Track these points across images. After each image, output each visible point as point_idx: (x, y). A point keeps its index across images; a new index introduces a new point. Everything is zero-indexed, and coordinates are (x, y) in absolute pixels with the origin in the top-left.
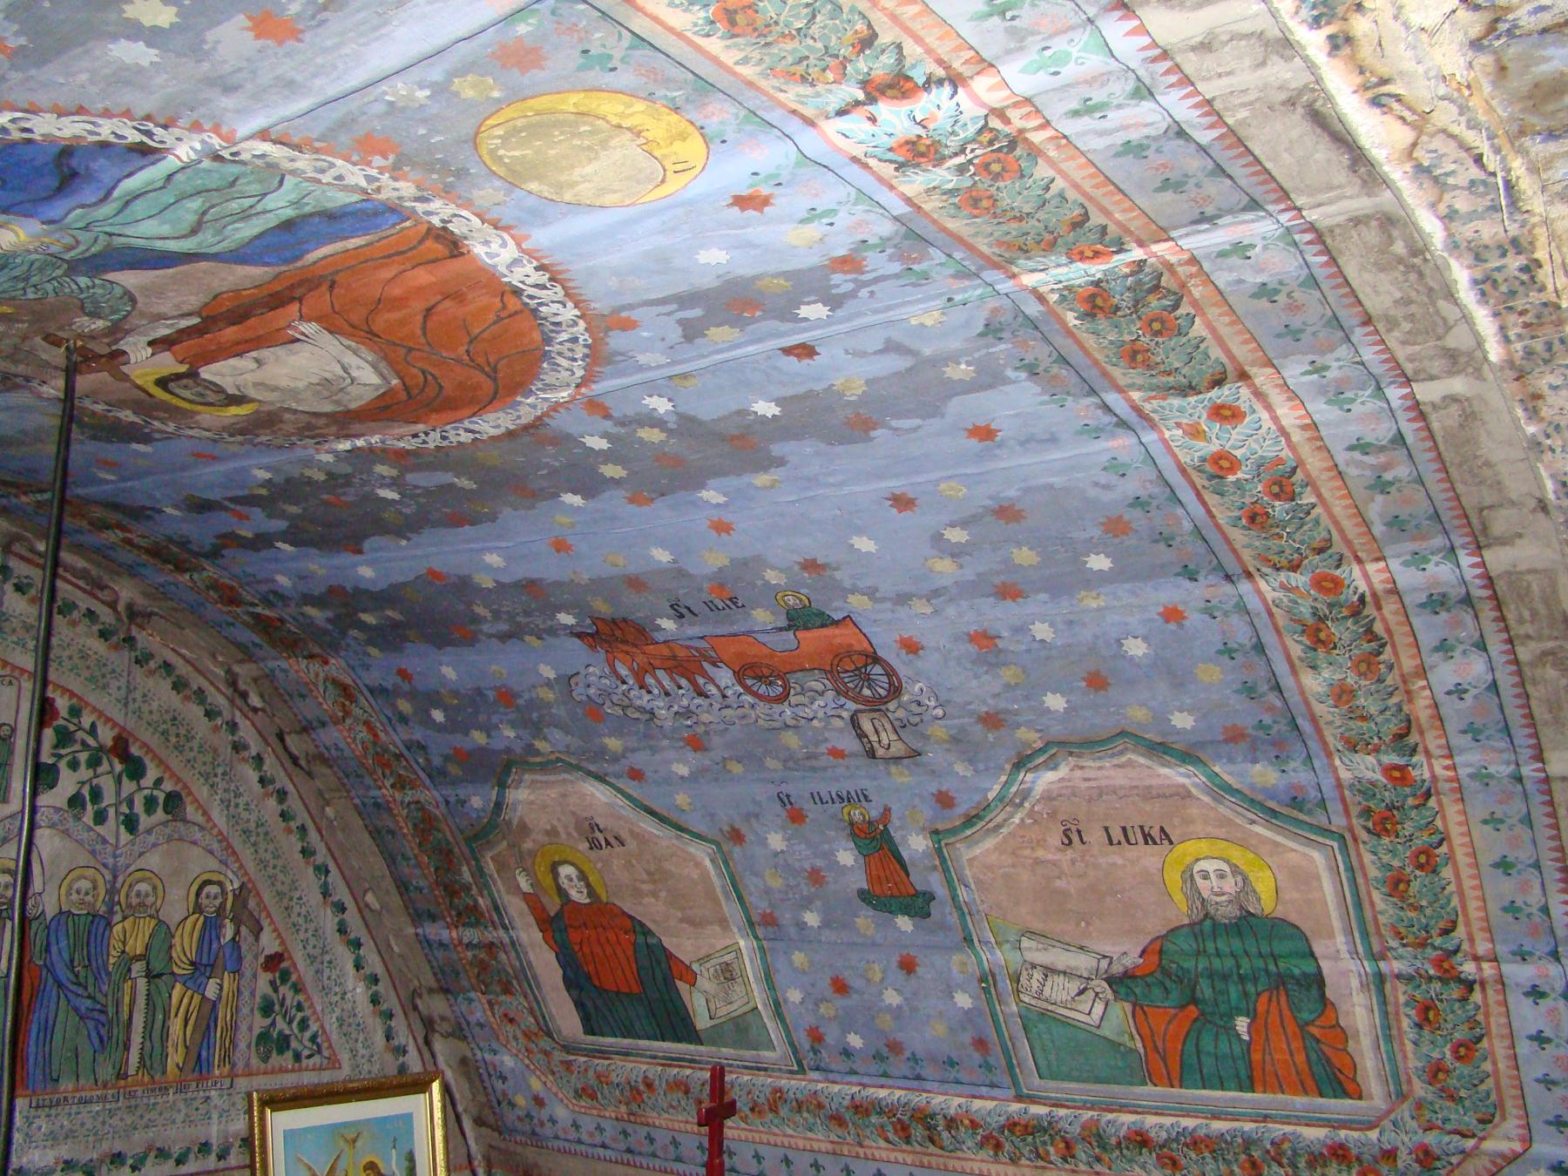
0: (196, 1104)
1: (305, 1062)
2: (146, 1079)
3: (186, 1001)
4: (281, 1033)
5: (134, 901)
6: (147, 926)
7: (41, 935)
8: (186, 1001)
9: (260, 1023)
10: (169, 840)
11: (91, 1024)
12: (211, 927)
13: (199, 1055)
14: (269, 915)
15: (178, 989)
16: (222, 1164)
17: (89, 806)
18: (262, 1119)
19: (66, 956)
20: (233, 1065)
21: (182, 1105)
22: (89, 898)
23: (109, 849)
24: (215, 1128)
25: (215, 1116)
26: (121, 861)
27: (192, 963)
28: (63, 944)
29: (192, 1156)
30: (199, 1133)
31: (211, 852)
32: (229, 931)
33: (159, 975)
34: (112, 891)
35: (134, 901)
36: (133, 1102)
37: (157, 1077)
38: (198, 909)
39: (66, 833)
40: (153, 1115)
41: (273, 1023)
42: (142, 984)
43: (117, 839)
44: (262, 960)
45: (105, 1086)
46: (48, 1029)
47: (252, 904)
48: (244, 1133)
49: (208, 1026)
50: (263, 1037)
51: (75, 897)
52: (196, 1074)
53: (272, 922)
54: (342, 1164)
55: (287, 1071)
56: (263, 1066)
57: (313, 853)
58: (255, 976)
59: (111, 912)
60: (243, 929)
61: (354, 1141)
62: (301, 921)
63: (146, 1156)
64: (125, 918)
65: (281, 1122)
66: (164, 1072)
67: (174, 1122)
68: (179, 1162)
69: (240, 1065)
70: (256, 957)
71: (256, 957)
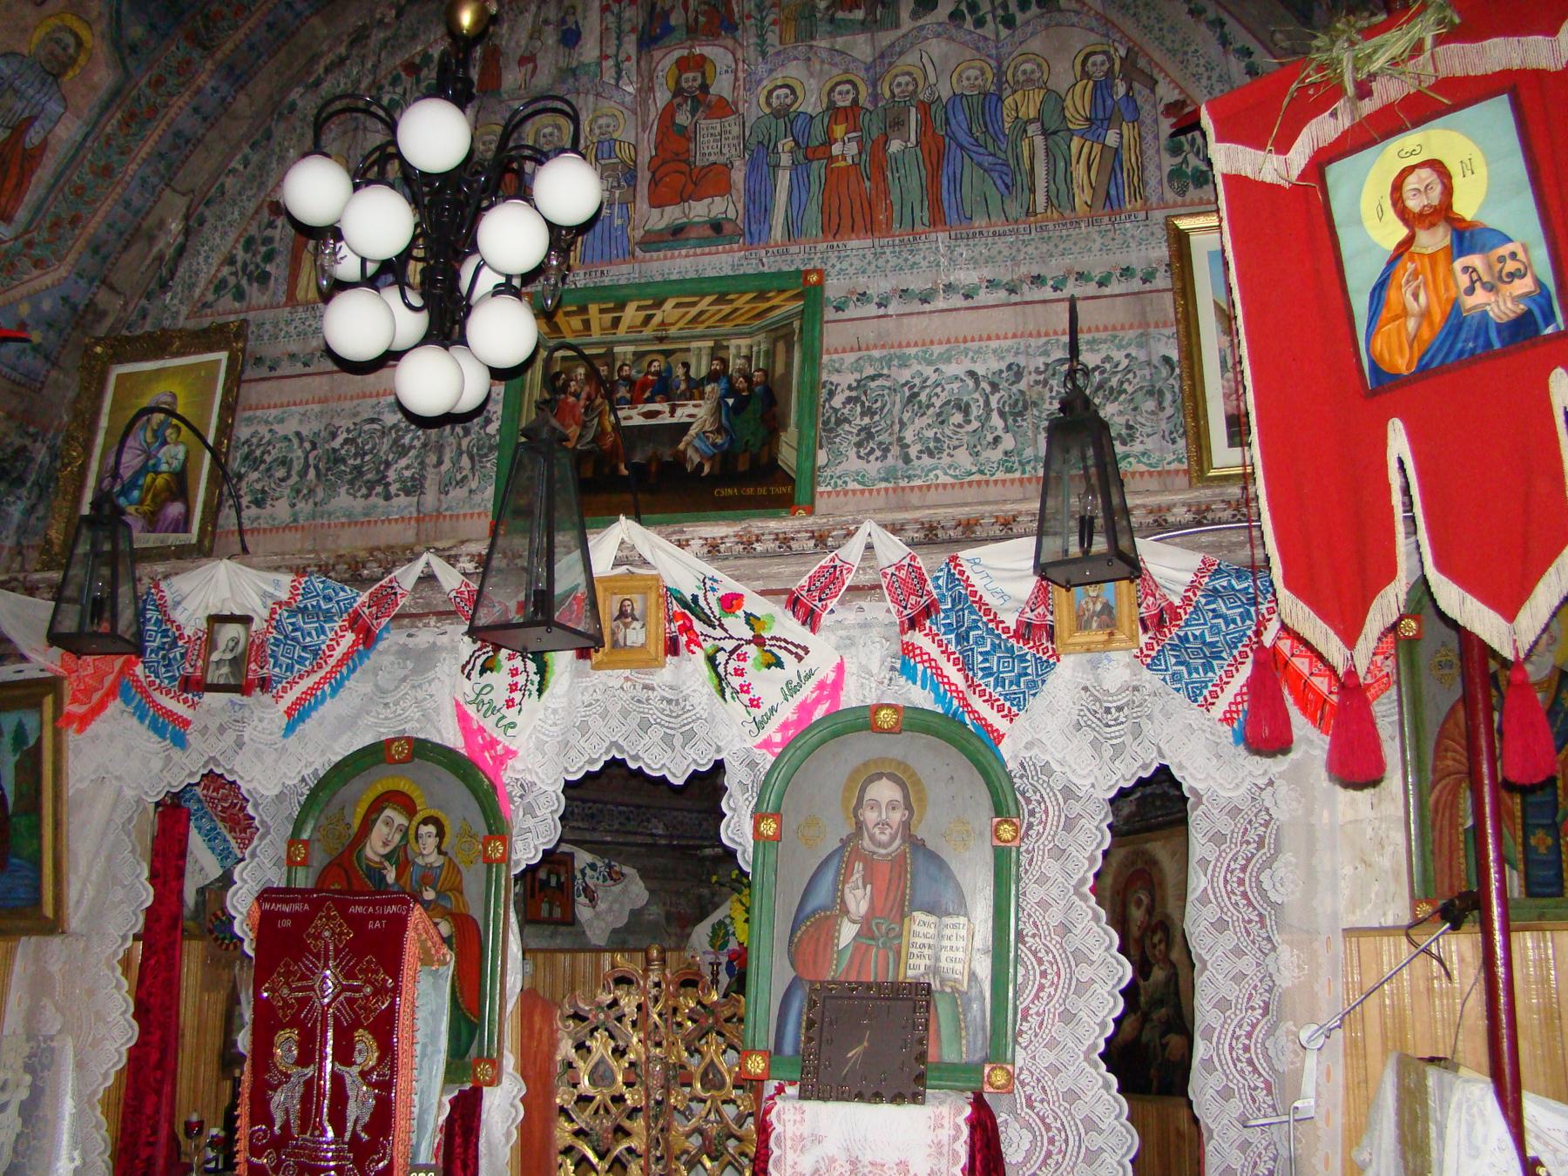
2: (1056, 215)
3: (1085, 150)
4: (1196, 169)
5: (1021, 78)
6: (1037, 97)
7: (940, 116)
8: (1085, 150)
9: (1169, 162)
10: (1047, 26)
11: (995, 175)
12: (1102, 88)
13: (1108, 195)
14: (1162, 70)
15: (1075, 143)
17: (968, 17)
19: (964, 126)
20: (1146, 200)
21: (1096, 236)
22: (979, 81)
23: (991, 44)
26: (1003, 50)
27: (1087, 119)
28: (961, 117)
30: (1122, 259)
31: (1092, 30)
32: (1121, 89)
33: (1055, 133)
34: (1000, 74)
35: (1021, 78)
37: (1067, 213)
38: (1085, 74)
39: (951, 39)
40: (1067, 245)
41: (1185, 160)
42: (1039, 141)
43: (997, 35)
44: (1161, 108)
45: (1016, 221)
46: (956, 182)
47: (1142, 63)
49: (1113, 169)
50: (1176, 174)
51: (965, 83)
52: (1108, 209)
53: (1167, 75)
56: (1179, 199)
57: (1205, 11)
58: (1156, 121)
59: (1000, 89)
60: (1136, 85)
62: (1201, 70)
63: (1065, 279)
64: (1014, 92)
66: (1073, 209)
67: (1090, 250)
68: (1101, 284)
69: (1154, 200)
70: (1155, 106)
71: (1155, 106)
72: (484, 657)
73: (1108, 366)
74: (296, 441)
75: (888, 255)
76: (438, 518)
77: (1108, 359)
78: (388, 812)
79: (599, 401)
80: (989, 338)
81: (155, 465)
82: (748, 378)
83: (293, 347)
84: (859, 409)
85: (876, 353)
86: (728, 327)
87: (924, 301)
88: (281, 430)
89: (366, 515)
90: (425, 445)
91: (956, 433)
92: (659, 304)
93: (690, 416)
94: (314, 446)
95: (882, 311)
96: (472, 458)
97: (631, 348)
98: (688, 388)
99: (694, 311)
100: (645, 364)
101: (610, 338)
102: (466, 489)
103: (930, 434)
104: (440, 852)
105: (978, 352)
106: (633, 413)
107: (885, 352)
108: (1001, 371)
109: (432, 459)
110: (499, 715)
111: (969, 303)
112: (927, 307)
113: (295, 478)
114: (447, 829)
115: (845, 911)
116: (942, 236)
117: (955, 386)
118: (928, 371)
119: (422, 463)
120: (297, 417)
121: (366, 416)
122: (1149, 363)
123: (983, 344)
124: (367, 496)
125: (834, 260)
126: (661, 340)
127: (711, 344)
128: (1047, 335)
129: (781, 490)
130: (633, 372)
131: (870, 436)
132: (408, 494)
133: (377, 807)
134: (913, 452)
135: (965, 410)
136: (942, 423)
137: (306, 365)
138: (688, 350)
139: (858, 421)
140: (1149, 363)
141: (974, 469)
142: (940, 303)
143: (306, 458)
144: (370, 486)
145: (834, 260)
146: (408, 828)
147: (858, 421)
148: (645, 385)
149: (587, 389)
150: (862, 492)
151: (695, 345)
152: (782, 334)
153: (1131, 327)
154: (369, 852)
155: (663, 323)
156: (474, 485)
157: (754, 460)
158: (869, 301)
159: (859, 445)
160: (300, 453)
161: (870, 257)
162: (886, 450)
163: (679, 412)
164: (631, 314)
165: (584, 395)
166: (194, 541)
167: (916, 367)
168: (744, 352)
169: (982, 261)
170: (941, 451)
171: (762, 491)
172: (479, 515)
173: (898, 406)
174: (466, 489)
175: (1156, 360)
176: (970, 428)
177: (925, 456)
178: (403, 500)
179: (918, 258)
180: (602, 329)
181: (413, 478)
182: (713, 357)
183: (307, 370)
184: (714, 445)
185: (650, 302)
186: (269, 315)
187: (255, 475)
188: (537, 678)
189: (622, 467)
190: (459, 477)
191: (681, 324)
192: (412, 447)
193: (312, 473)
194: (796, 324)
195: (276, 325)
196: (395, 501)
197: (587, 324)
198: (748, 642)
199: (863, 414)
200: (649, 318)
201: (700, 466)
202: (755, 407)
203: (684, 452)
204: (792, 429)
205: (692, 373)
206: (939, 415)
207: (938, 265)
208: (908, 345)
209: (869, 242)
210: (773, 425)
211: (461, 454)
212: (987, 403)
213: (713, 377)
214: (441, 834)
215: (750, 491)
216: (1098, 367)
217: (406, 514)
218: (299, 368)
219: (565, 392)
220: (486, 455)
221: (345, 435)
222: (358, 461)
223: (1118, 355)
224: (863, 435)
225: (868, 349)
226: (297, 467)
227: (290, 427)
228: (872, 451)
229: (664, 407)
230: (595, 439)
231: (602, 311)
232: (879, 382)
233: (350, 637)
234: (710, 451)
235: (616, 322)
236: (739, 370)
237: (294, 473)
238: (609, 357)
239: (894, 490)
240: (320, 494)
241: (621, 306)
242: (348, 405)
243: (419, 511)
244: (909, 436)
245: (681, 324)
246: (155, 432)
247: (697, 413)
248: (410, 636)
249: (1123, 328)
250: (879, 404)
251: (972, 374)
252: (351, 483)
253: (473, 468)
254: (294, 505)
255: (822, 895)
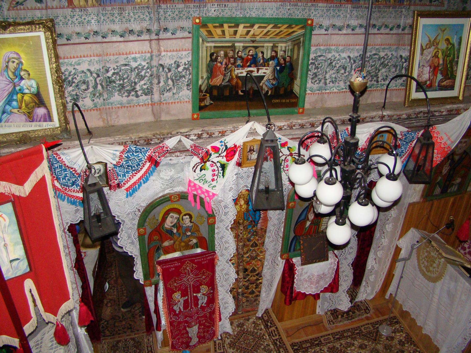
0: (398, 12)
1: (433, 3)
2: (384, 3)
16: (403, 32)
18: (417, 20)
21: (393, 12)
24: (402, 21)
25: (403, 17)
29: (394, 29)
36: (380, 10)
40: (385, 14)
48: (411, 23)
54: (438, 38)
55: (427, 5)
56: (419, 3)
61: (444, 31)
63: (382, 26)
65: (423, 21)
68: (391, 30)
72: (201, 165)
73: (386, 57)
74: (89, 74)
75: (331, 11)
76: (160, 104)
77: (386, 55)
78: (171, 214)
79: (230, 66)
80: (356, 45)
81: (20, 90)
82: (285, 59)
83: (78, 29)
84: (314, 67)
85: (322, 48)
86: (278, 39)
87: (340, 30)
88: (80, 68)
89: (128, 103)
90: (151, 75)
91: (341, 76)
92: (252, 26)
93: (264, 73)
94: (98, 76)
95: (326, 32)
96: (173, 81)
97: (242, 44)
98: (264, 62)
99: (266, 30)
100: (247, 51)
101: (233, 39)
102: (171, 93)
103: (334, 76)
104: (191, 222)
105: (352, 50)
106: (243, 71)
107: (325, 47)
108: (357, 57)
109: (155, 81)
110: (209, 184)
111: (353, 32)
112: (340, 32)
113: (91, 89)
114: (193, 216)
115: (308, 219)
116: (350, 6)
117: (344, 60)
118: (337, 55)
119: (151, 83)
120: (87, 63)
121: (122, 63)
122: (396, 57)
123: (354, 47)
124: (128, 96)
125: (313, 11)
126: (253, 42)
127: (272, 45)
128: (372, 45)
129: (294, 100)
130: (243, 54)
131: (316, 76)
132: (146, 95)
133: (167, 213)
134: (328, 82)
135: (345, 68)
136: (338, 73)
137: (86, 38)
138: (263, 47)
139: (313, 71)
140: (396, 57)
141: (344, 88)
142: (344, 32)
143: (95, 80)
144: (129, 92)
145: (313, 11)
146: (179, 218)
147: (313, 71)
148: (248, 60)
149: (225, 60)
150: (311, 94)
151: (266, 45)
152: (297, 43)
153: (395, 45)
154: (166, 226)
155: (254, 35)
156: (175, 91)
157: (286, 89)
158: (322, 28)
159: (312, 79)
160: (91, 78)
161: (325, 11)
162: (320, 81)
163: (260, 71)
164: (241, 29)
165: (224, 63)
166: (58, 125)
167: (333, 53)
168: (283, 49)
169: (360, 17)
170: (336, 81)
171: (288, 101)
172: (178, 102)
173: (326, 66)
174: (171, 93)
175: (398, 56)
176: (345, 75)
177: (331, 83)
178: (144, 97)
179: (340, 13)
180: (230, 35)
181: (147, 88)
182: (272, 50)
183: (87, 41)
184: (272, 84)
185: (249, 25)
186: (60, 12)
187: (71, 89)
188: (222, 171)
189: (240, 92)
190: (168, 88)
191: (261, 36)
192: (145, 76)
193: (99, 87)
194: (302, 39)
195: (65, 18)
196: (141, 98)
197: (223, 32)
198: (288, 156)
199: (315, 69)
200: (248, 32)
201: (268, 92)
202: (286, 71)
203: (262, 87)
204: (298, 79)
205: (265, 56)
206: (337, 70)
207: (346, 17)
208: (332, 45)
209: (325, 4)
210: (292, 78)
211: (168, 79)
212: (352, 67)
213: (272, 58)
214: (191, 217)
215: (284, 101)
216: (383, 57)
217: (146, 102)
218: (83, 40)
219: (216, 61)
220: (179, 80)
221: (113, 71)
222: (121, 82)
223: (389, 54)
224: (314, 75)
225: (320, 46)
226: (91, 84)
227: (84, 67)
228: (316, 81)
229: (254, 69)
230: (229, 81)
231: (230, 27)
232: (322, 58)
233: (148, 164)
234: (271, 86)
235: (235, 32)
236: (282, 56)
237: (90, 87)
238: (233, 47)
239: (321, 94)
240: (105, 96)
241: (237, 26)
242: (112, 58)
243: (152, 101)
244: (327, 76)
245: (261, 36)
246: (14, 73)
247: (266, 72)
248: (170, 160)
249: (393, 45)
250: (320, 65)
251: (349, 57)
252: (120, 91)
253: (173, 85)
254: (94, 100)
255: (303, 217)
